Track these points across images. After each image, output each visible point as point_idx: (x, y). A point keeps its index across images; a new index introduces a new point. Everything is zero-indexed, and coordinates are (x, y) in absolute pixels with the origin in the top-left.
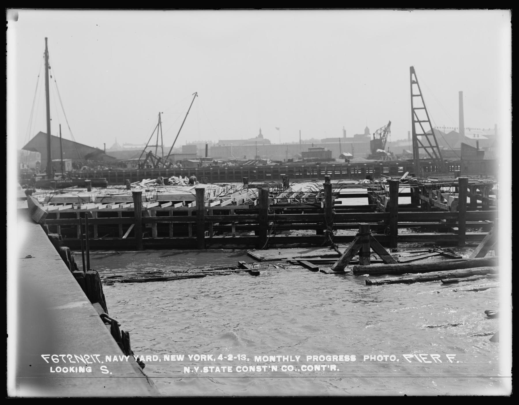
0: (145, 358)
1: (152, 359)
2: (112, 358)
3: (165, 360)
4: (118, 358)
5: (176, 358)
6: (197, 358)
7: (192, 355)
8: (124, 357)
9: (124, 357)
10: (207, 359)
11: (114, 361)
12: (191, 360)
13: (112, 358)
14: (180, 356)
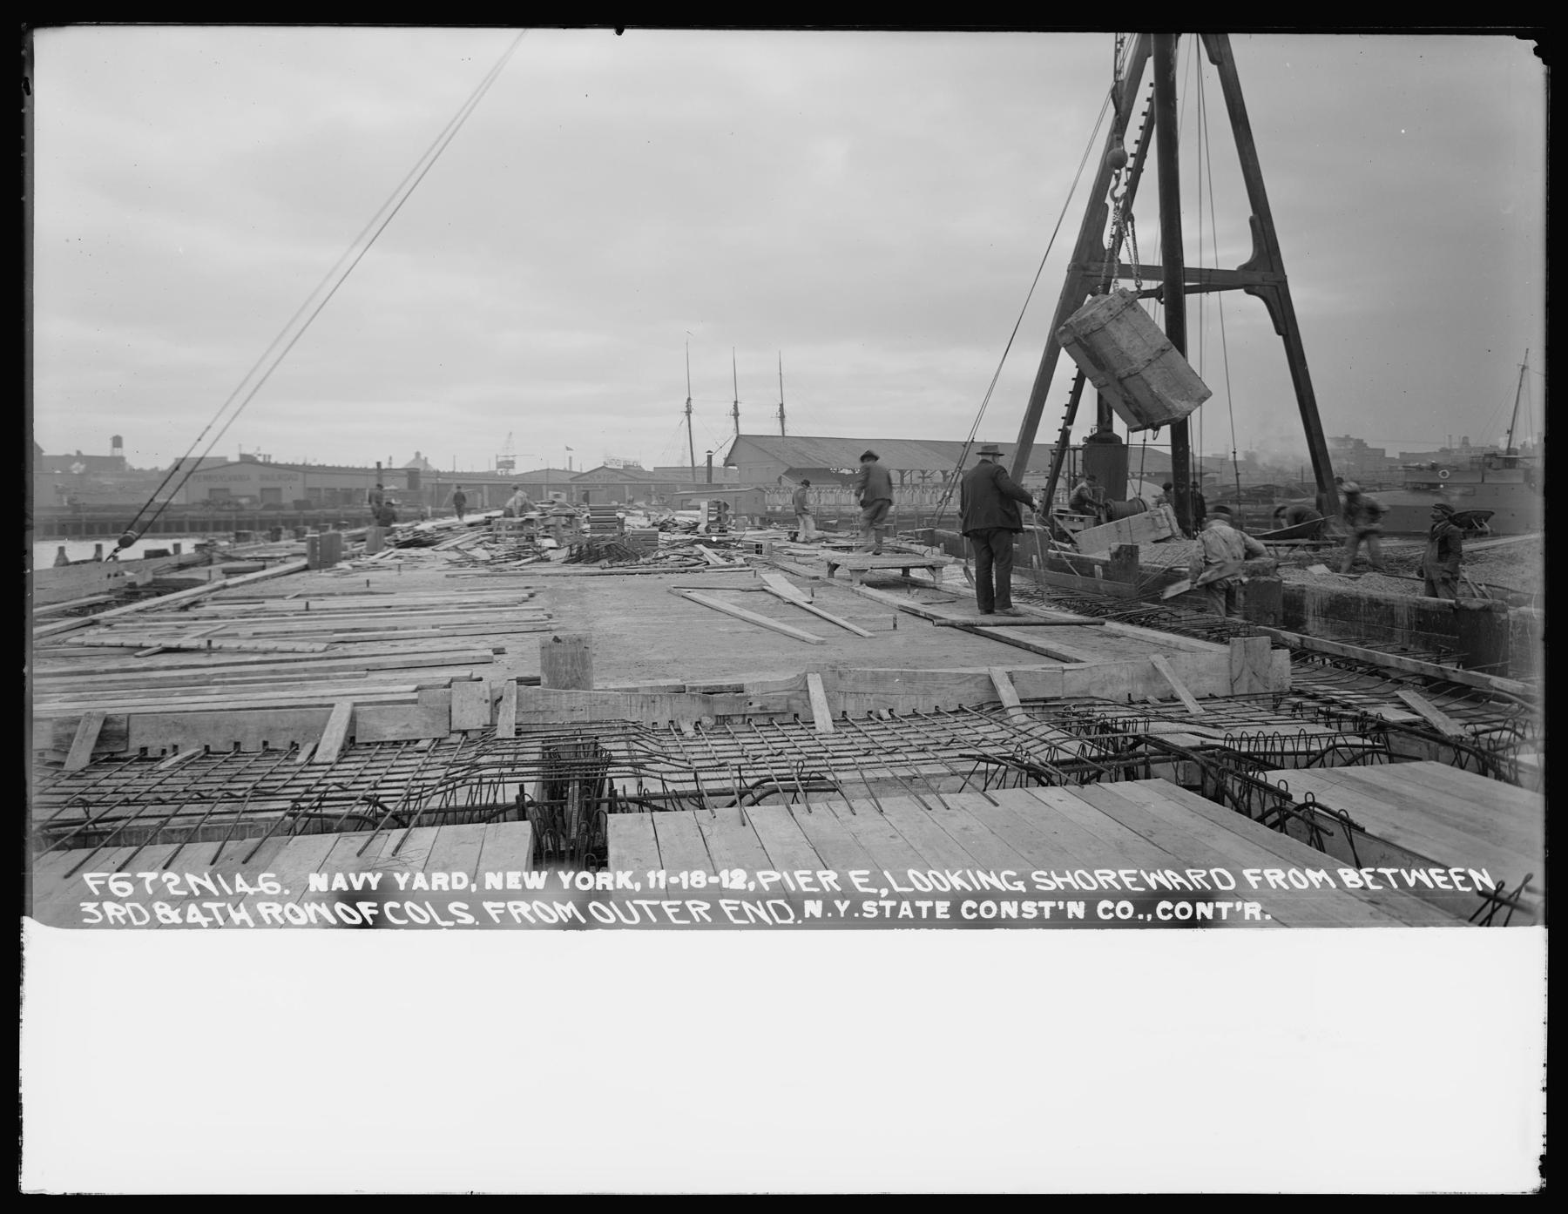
0: (429, 880)
1: (450, 883)
3: (488, 887)
4: (349, 883)
5: (522, 881)
6: (585, 881)
7: (571, 873)
8: (366, 880)
9: (366, 880)
10: (614, 883)
11: (334, 889)
12: (566, 886)
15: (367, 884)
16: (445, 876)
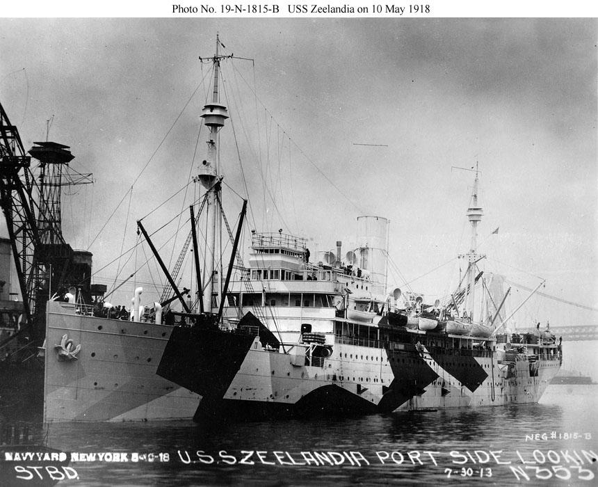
0: (50, 456)
2: (14, 457)
5: (86, 457)
6: (108, 457)
7: (103, 454)
8: (28, 456)
13: (14, 457)
14: (91, 454)
15: (28, 456)
16: (57, 454)
